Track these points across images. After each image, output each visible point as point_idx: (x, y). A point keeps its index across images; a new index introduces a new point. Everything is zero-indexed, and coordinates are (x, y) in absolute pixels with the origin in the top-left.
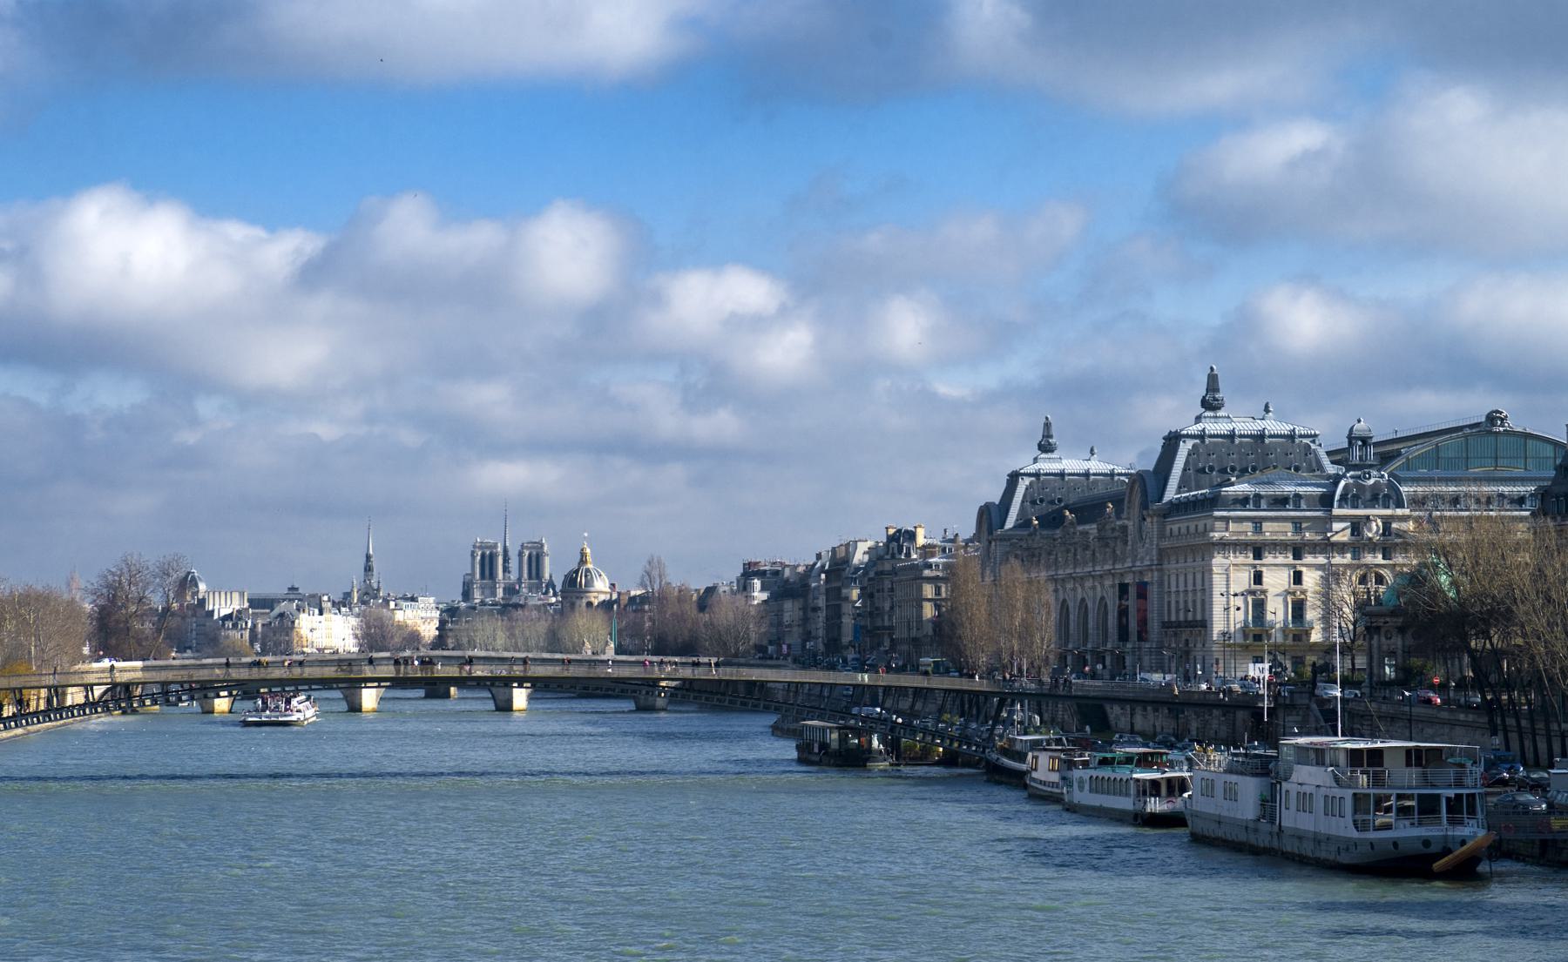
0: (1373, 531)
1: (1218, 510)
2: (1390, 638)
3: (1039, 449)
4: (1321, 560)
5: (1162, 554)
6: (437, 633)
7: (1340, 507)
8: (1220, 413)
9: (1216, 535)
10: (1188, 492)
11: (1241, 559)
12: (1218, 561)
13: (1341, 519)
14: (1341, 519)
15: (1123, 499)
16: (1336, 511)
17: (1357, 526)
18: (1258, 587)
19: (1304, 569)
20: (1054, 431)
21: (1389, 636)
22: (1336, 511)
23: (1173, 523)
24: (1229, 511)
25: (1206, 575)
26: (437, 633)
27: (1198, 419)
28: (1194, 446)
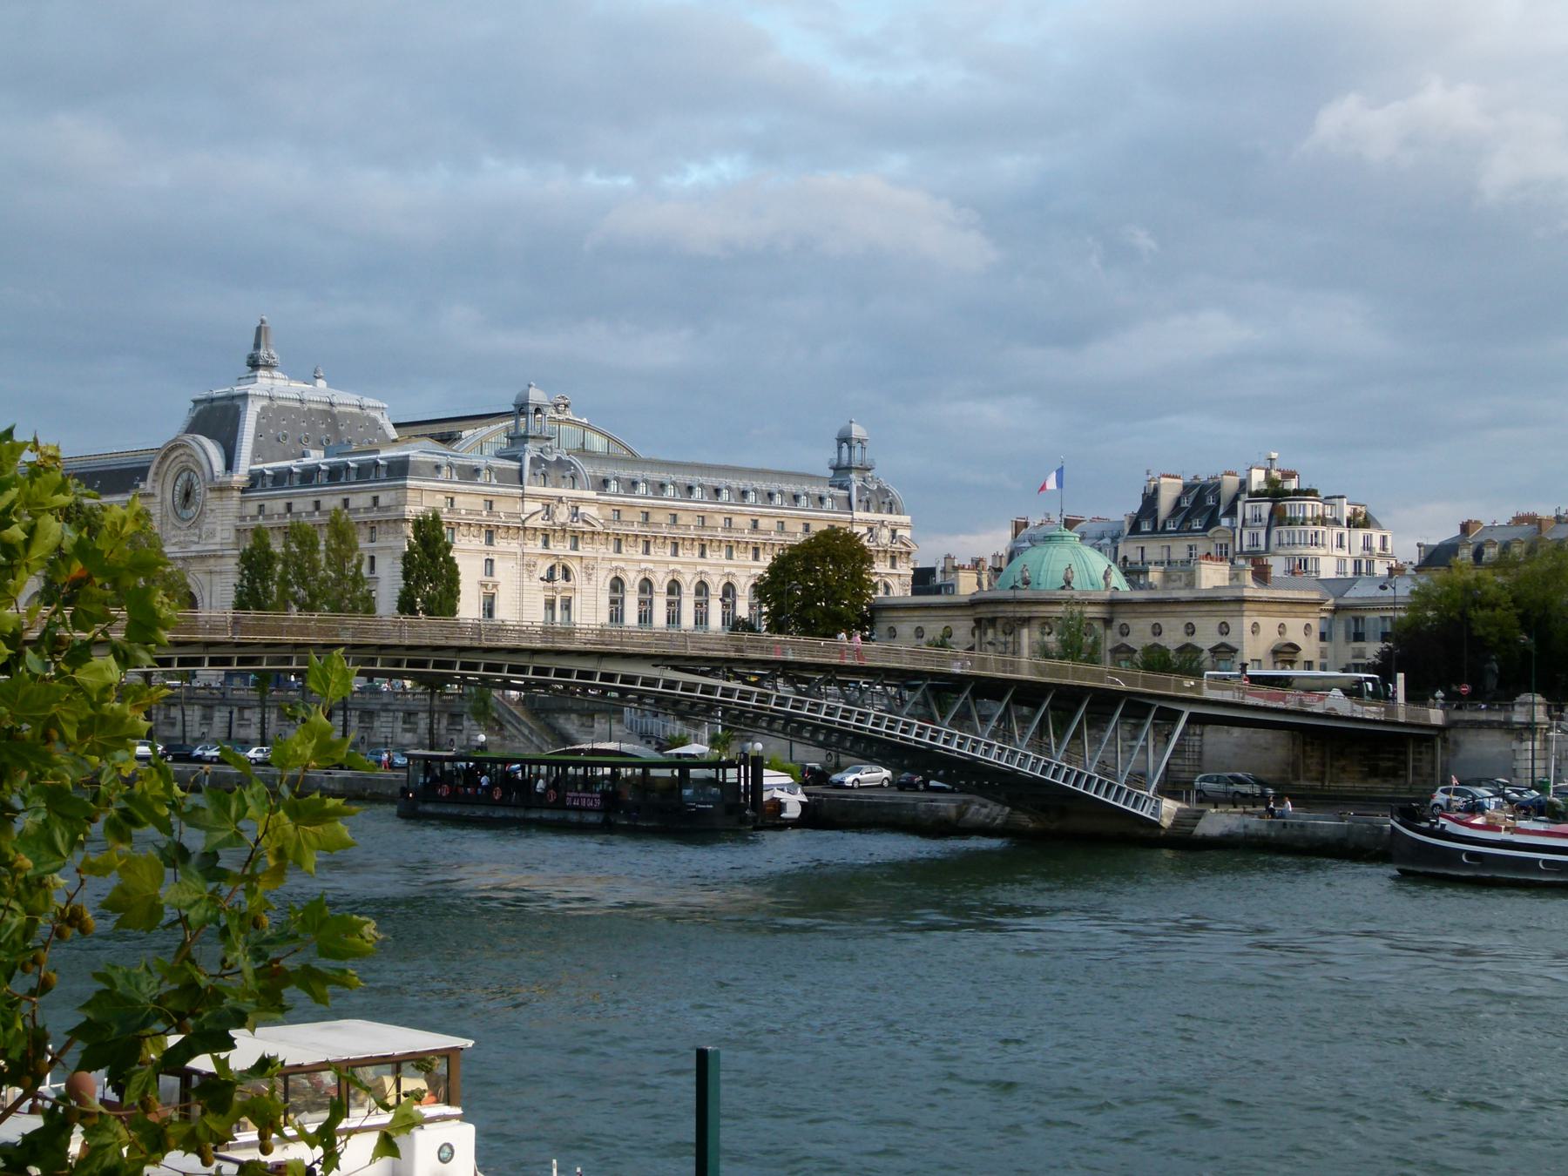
0: (562, 515)
1: (412, 479)
2: (1049, 634)
4: (514, 546)
6: (451, 554)
7: (529, 484)
8: (276, 373)
9: (412, 508)
10: (263, 463)
13: (534, 497)
14: (534, 497)
15: (148, 468)
16: (529, 489)
19: (495, 557)
21: (1047, 630)
22: (529, 489)
24: (424, 480)
26: (451, 554)
28: (263, 408)
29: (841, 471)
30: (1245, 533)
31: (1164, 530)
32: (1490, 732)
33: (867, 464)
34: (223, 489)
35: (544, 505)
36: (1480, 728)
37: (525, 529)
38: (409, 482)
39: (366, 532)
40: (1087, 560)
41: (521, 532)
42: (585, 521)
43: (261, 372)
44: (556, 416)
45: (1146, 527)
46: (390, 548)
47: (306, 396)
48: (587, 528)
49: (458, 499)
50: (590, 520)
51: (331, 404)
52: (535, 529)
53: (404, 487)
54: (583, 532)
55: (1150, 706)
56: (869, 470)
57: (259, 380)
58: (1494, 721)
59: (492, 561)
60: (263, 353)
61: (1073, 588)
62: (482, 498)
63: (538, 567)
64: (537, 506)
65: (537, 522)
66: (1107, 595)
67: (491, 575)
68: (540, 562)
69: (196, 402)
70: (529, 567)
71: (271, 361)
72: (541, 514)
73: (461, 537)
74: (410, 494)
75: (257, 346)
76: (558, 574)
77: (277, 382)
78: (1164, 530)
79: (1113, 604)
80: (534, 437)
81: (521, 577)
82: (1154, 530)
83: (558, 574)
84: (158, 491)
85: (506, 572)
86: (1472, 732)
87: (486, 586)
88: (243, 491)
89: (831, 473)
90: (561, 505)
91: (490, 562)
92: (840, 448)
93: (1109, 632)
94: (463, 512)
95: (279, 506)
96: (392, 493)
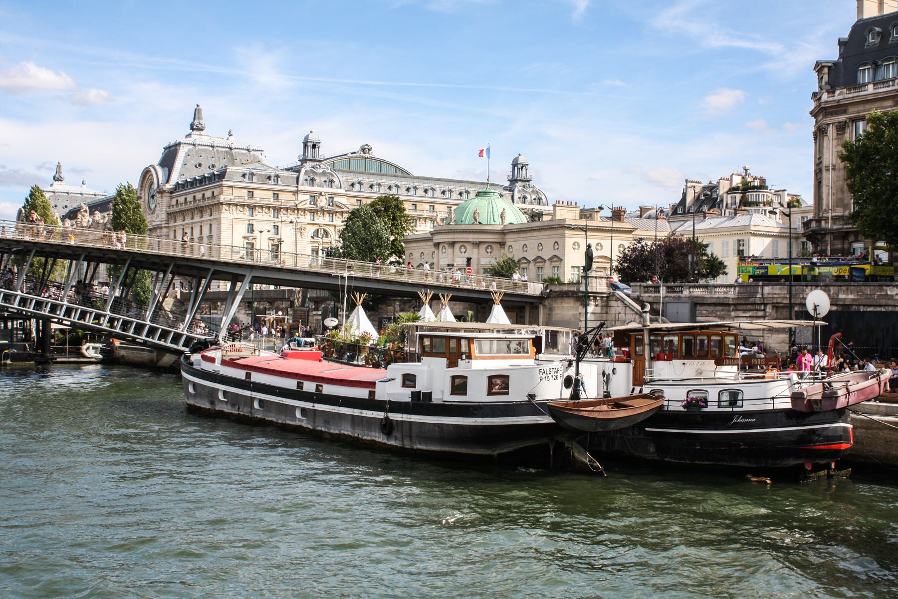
3: (54, 179)
5: (172, 216)
7: (303, 185)
8: (202, 133)
11: (241, 215)
12: (226, 215)
13: (305, 192)
14: (305, 192)
16: (301, 188)
17: (314, 197)
18: (250, 235)
20: (62, 170)
23: (180, 196)
25: (214, 227)
27: (189, 136)
28: (189, 150)
29: (513, 181)
30: (727, 212)
31: (689, 212)
32: (567, 300)
33: (528, 178)
34: (161, 192)
35: (311, 196)
36: (562, 297)
37: (298, 210)
38: (224, 183)
39: (209, 211)
40: (494, 206)
41: (296, 211)
42: (337, 206)
43: (195, 132)
44: (364, 155)
45: (680, 211)
46: (216, 219)
47: (215, 144)
48: (338, 209)
49: (256, 192)
50: (340, 205)
51: (231, 149)
52: (305, 210)
53: (221, 186)
54: (336, 212)
55: (209, 270)
56: (529, 181)
57: (192, 136)
58: (571, 291)
59: (252, 225)
60: (196, 122)
61: (480, 223)
62: (272, 193)
63: (307, 230)
64: (307, 197)
65: (308, 206)
66: (500, 228)
67: (277, 234)
68: (308, 227)
69: (165, 149)
70: (301, 230)
71: (200, 126)
72: (308, 202)
73: (257, 213)
74: (225, 189)
75: (194, 119)
76: (321, 232)
77: (202, 137)
78: (689, 212)
79: (503, 233)
80: (310, 160)
81: (296, 235)
82: (684, 213)
83: (321, 232)
84: (142, 196)
85: (287, 233)
86: (559, 300)
87: (273, 240)
88: (171, 192)
89: (509, 183)
90: (321, 197)
91: (276, 227)
92: (513, 169)
93: (502, 251)
94: (258, 199)
95: (190, 198)
96: (218, 189)
